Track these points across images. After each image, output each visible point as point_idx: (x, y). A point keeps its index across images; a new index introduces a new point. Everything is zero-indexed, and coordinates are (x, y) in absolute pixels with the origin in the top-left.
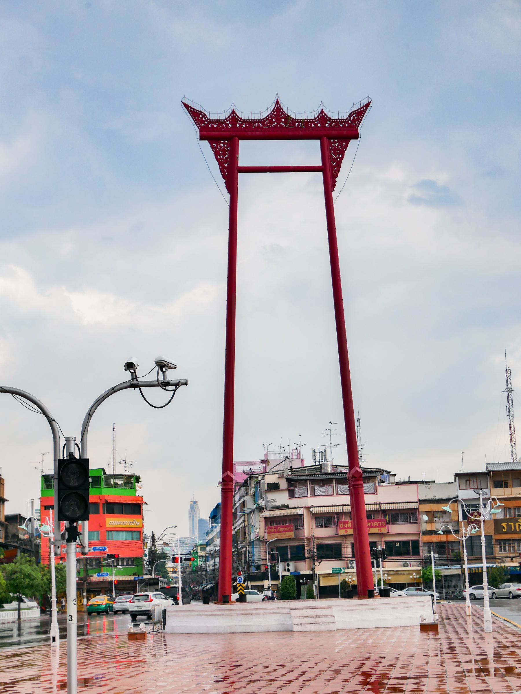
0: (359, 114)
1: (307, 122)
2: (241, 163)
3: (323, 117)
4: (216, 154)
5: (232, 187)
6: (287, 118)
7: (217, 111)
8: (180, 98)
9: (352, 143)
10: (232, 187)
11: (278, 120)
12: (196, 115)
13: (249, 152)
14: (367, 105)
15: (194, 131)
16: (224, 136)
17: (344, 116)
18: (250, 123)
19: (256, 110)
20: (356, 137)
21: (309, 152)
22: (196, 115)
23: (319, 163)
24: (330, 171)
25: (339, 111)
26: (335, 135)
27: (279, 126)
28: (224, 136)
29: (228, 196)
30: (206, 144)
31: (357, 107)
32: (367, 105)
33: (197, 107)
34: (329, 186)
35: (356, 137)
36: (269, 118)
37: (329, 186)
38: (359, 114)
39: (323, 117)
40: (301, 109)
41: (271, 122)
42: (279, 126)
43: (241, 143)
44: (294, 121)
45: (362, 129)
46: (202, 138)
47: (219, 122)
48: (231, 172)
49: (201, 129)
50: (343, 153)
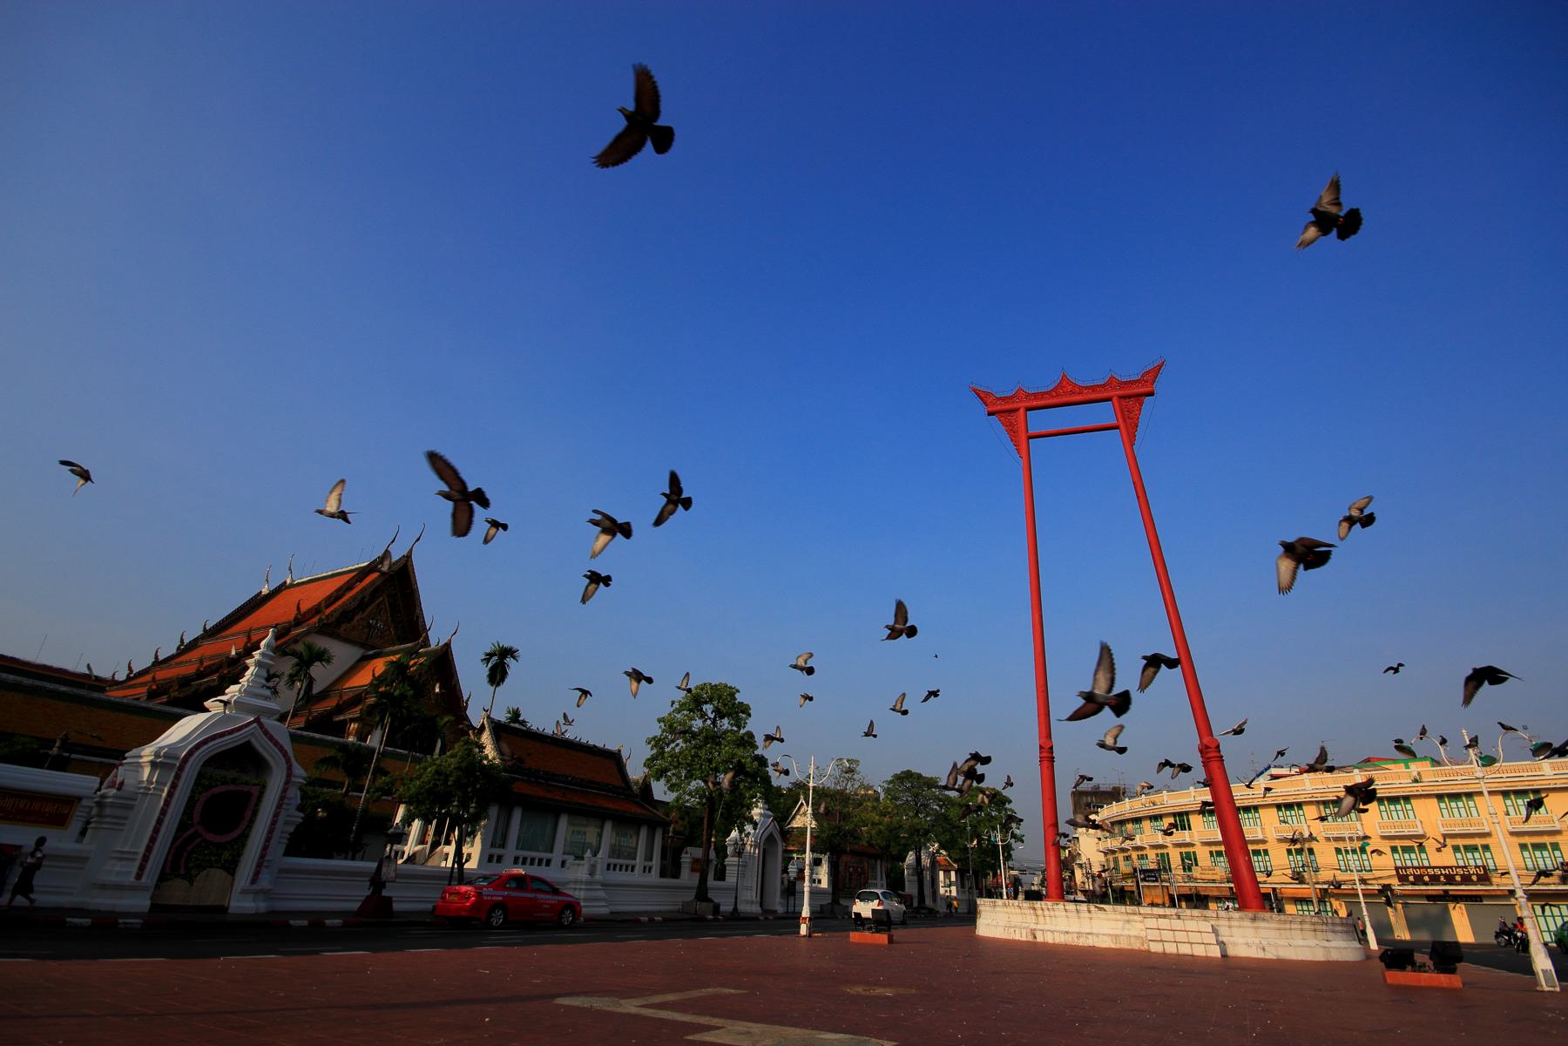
2: (1032, 431)
7: (1002, 388)
13: (1039, 421)
15: (984, 410)
27: (1066, 395)
32: (1160, 366)
36: (1055, 390)
40: (1088, 375)
42: (1066, 395)
45: (1157, 387)
46: (990, 414)
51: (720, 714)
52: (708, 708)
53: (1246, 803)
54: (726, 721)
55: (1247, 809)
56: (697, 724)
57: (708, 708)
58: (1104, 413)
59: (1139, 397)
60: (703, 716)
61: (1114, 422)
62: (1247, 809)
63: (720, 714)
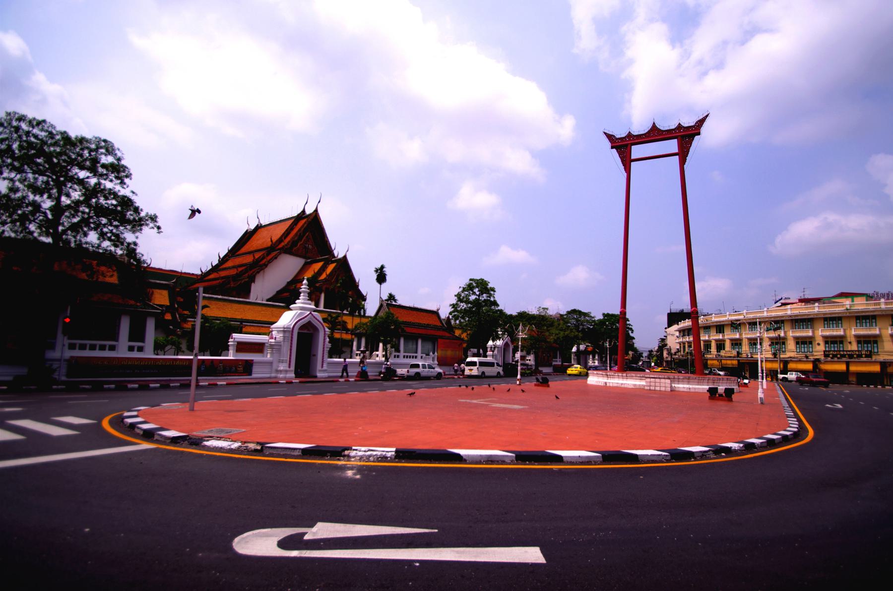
0: (701, 122)
5: (628, 169)
7: (620, 133)
8: (602, 130)
9: (696, 137)
10: (628, 169)
12: (610, 137)
13: (637, 151)
14: (707, 116)
15: (609, 144)
16: (623, 146)
17: (693, 124)
20: (699, 134)
21: (672, 146)
22: (610, 137)
23: (677, 151)
24: (683, 154)
25: (688, 121)
26: (685, 136)
28: (623, 146)
29: (625, 174)
30: (614, 150)
31: (701, 117)
32: (707, 116)
34: (682, 162)
35: (699, 134)
36: (649, 132)
37: (682, 162)
38: (701, 122)
40: (665, 125)
42: (655, 134)
43: (633, 147)
45: (703, 130)
47: (621, 139)
48: (627, 161)
51: (482, 293)
52: (476, 290)
54: (484, 295)
56: (473, 298)
57: (476, 290)
60: (474, 293)
61: (677, 151)
63: (482, 293)
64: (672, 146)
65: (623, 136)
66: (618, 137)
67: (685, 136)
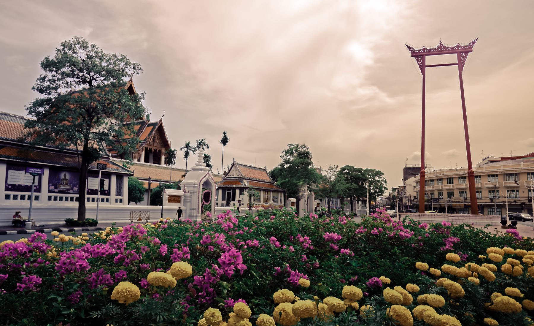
0: (473, 43)
1: (452, 48)
3: (458, 46)
4: (418, 61)
5: (423, 72)
6: (444, 47)
7: (417, 47)
10: (423, 72)
11: (441, 47)
12: (410, 48)
13: (429, 60)
15: (409, 54)
16: (419, 55)
18: (430, 50)
19: (433, 45)
22: (410, 48)
25: (465, 43)
26: (463, 52)
27: (441, 50)
28: (419, 55)
31: (473, 40)
33: (411, 46)
35: (471, 51)
39: (458, 46)
41: (438, 49)
42: (441, 50)
44: (447, 48)
45: (474, 48)
48: (423, 67)
49: (412, 53)
50: (466, 57)
53: (477, 175)
55: (476, 177)
58: (453, 58)
59: (467, 52)
62: (476, 177)
64: (453, 58)
65: (420, 49)
66: (416, 49)
67: (463, 52)
